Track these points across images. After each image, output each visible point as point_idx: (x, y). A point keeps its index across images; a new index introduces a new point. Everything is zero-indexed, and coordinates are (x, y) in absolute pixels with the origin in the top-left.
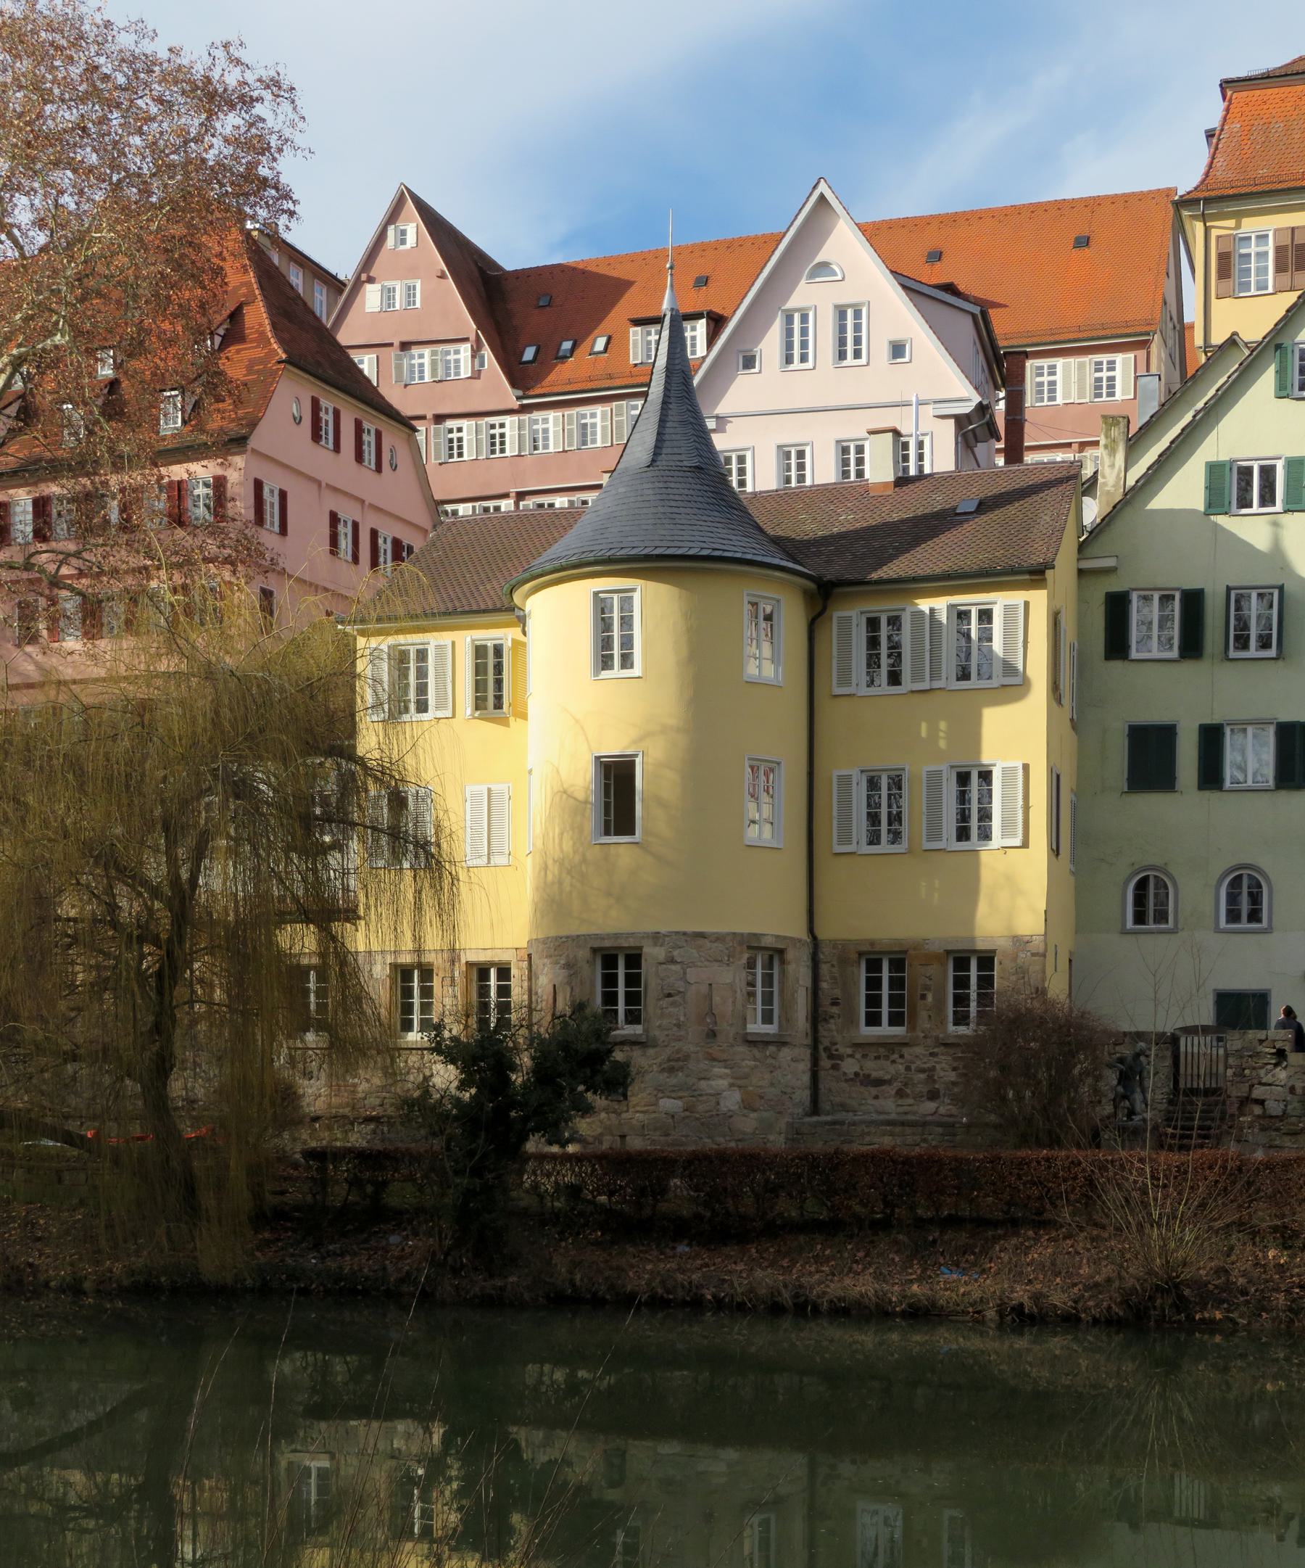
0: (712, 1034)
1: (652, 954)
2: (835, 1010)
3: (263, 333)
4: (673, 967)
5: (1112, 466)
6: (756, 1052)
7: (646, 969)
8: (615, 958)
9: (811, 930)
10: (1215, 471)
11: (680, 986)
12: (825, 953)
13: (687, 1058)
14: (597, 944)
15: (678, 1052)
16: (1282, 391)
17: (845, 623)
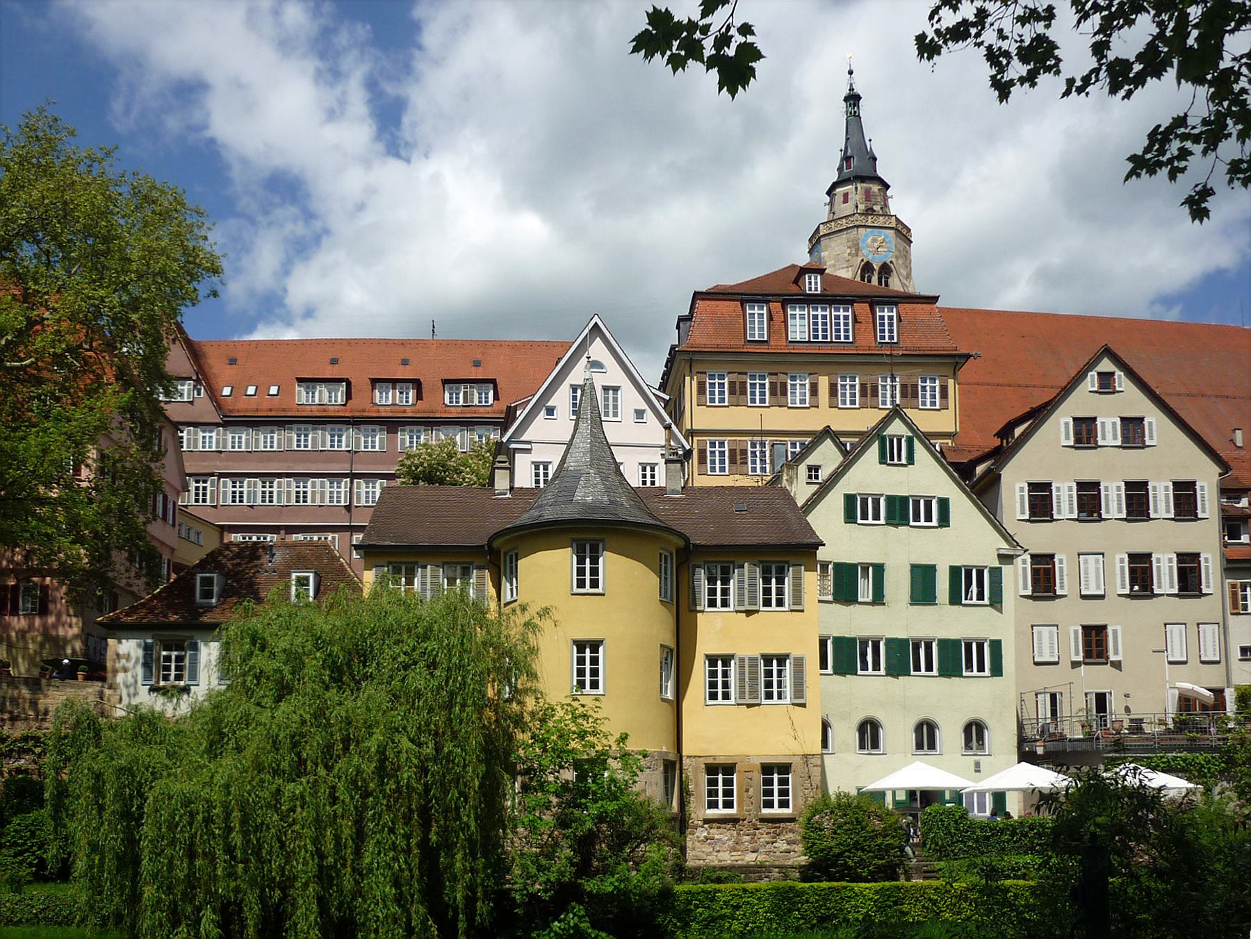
10: (850, 500)
16: (882, 461)
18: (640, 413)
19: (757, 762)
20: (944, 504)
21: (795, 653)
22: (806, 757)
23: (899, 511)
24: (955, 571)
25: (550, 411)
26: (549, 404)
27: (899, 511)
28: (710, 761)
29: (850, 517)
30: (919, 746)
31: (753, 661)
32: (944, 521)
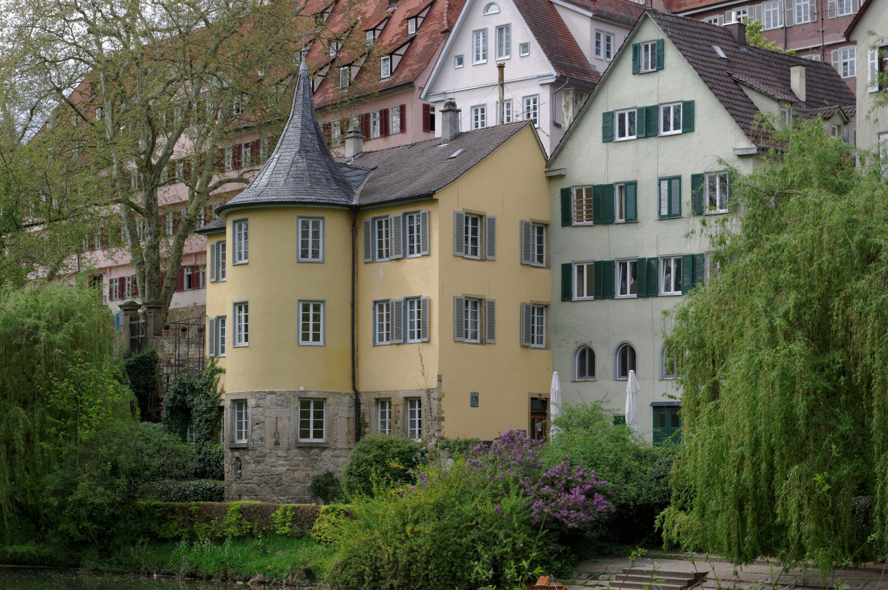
0: (277, 443)
1: (251, 402)
2: (367, 430)
3: (442, 14)
4: (260, 409)
5: (567, 117)
6: (303, 452)
7: (249, 410)
8: (309, 403)
9: (354, 388)
10: (608, 117)
11: (262, 418)
12: (363, 399)
13: (265, 456)
14: (235, 398)
15: (261, 452)
16: (636, 71)
17: (367, 223)
18: (525, 47)
19: (401, 396)
20: (689, 107)
21: (424, 295)
22: (429, 392)
23: (647, 122)
24: (697, 179)
25: (460, 61)
26: (459, 53)
27: (647, 122)
28: (377, 396)
29: (608, 137)
30: (582, 373)
31: (398, 303)
32: (689, 126)
